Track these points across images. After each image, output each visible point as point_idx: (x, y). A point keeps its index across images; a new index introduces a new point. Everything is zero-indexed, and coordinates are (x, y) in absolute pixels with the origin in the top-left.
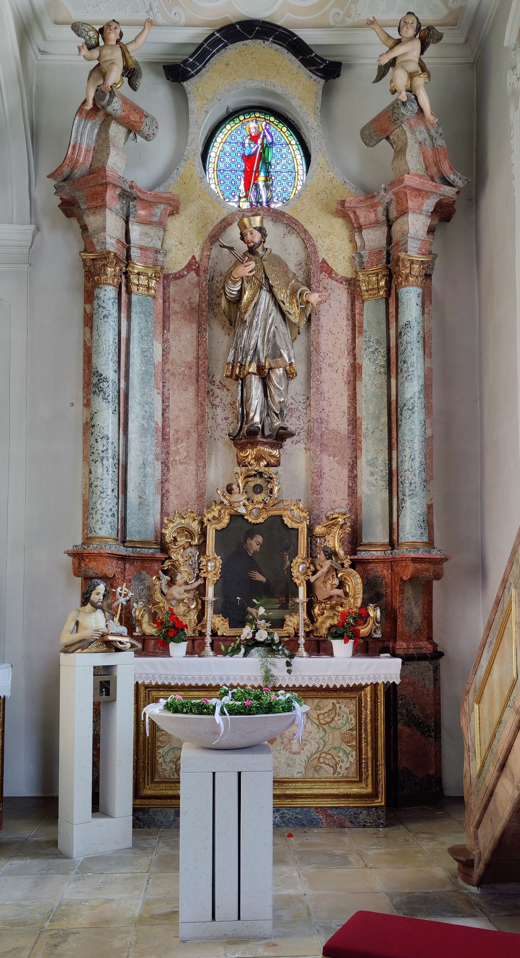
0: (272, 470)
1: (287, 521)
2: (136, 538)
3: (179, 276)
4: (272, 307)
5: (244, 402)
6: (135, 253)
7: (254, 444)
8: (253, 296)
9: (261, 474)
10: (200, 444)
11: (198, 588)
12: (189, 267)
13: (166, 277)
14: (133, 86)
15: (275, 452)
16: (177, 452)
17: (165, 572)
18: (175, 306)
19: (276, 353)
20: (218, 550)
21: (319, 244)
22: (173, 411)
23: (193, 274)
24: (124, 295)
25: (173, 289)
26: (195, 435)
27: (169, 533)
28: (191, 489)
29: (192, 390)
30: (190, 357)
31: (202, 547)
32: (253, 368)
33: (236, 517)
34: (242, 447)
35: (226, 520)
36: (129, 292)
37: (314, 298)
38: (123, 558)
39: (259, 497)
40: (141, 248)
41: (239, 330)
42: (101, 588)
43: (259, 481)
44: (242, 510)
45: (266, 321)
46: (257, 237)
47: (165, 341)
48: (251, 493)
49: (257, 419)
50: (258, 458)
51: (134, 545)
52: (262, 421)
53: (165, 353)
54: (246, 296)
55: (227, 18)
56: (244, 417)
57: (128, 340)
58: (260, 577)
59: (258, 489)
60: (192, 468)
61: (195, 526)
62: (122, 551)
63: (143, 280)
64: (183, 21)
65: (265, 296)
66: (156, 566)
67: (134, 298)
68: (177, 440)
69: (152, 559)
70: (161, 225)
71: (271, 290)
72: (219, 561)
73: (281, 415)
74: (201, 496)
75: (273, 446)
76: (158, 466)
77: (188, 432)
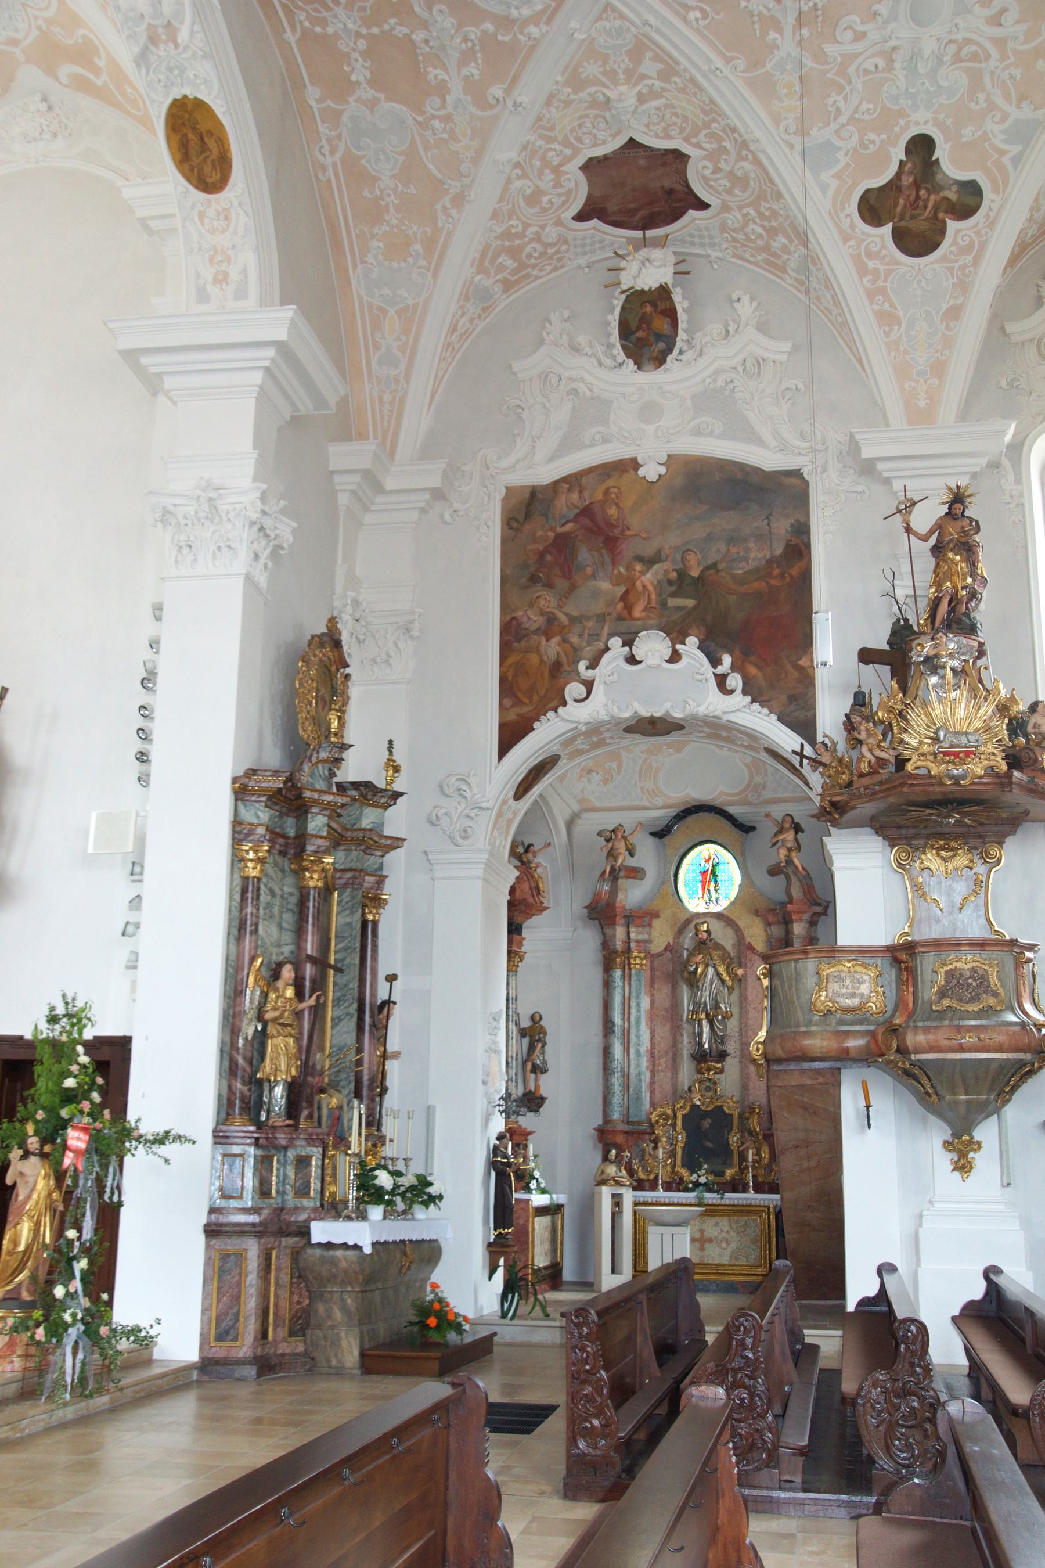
0: (717, 1076)
1: (725, 1109)
2: (635, 1119)
3: (660, 955)
4: (715, 977)
5: (700, 1034)
6: (633, 945)
7: (706, 1061)
8: (703, 971)
9: (710, 1080)
10: (674, 1060)
11: (672, 1151)
12: (666, 949)
13: (652, 956)
14: (632, 854)
15: (719, 1065)
16: (660, 1064)
17: (651, 1142)
18: (658, 974)
19: (716, 1007)
20: (684, 1128)
21: (746, 933)
22: (658, 1039)
23: (669, 953)
24: (627, 970)
25: (656, 963)
26: (671, 1054)
27: (654, 1118)
28: (668, 1087)
29: (668, 1025)
30: (667, 1005)
31: (674, 1126)
32: (703, 1016)
33: (694, 1107)
34: (699, 1063)
35: (688, 1109)
36: (630, 969)
37: (740, 972)
38: (626, 1133)
39: (710, 1094)
40: (638, 942)
41: (695, 990)
42: (614, 1152)
43: (708, 1084)
44: (698, 1103)
45: (711, 985)
46: (705, 935)
47: (652, 995)
48: (703, 1092)
49: (706, 1046)
50: (709, 1070)
51: (632, 1123)
52: (710, 1047)
53: (652, 1003)
54: (700, 970)
55: (687, 802)
56: (700, 1044)
57: (629, 998)
58: (710, 1145)
59: (708, 1089)
60: (669, 1074)
61: (670, 1112)
62: (627, 1128)
63: (638, 961)
64: (661, 804)
65: (711, 970)
66: (647, 1137)
67: (633, 972)
68: (660, 1058)
69: (644, 1133)
70: (650, 925)
71: (714, 966)
72: (684, 1134)
73: (722, 1043)
74: (675, 1092)
75: (718, 1062)
76: (648, 1074)
77: (667, 1052)
